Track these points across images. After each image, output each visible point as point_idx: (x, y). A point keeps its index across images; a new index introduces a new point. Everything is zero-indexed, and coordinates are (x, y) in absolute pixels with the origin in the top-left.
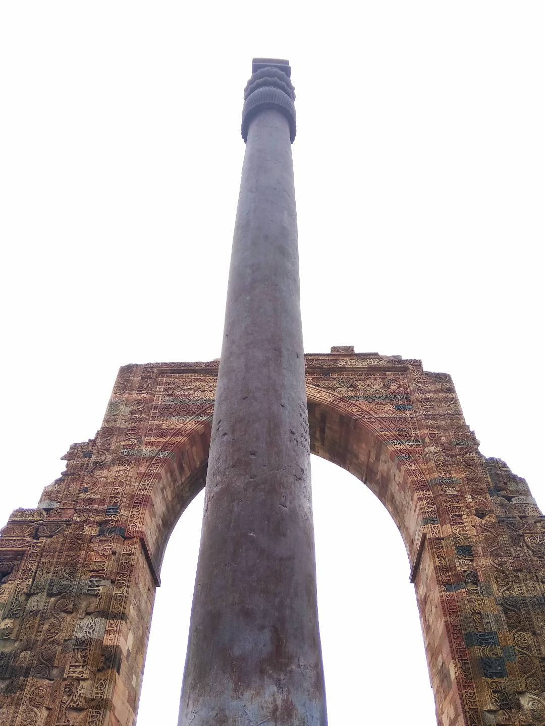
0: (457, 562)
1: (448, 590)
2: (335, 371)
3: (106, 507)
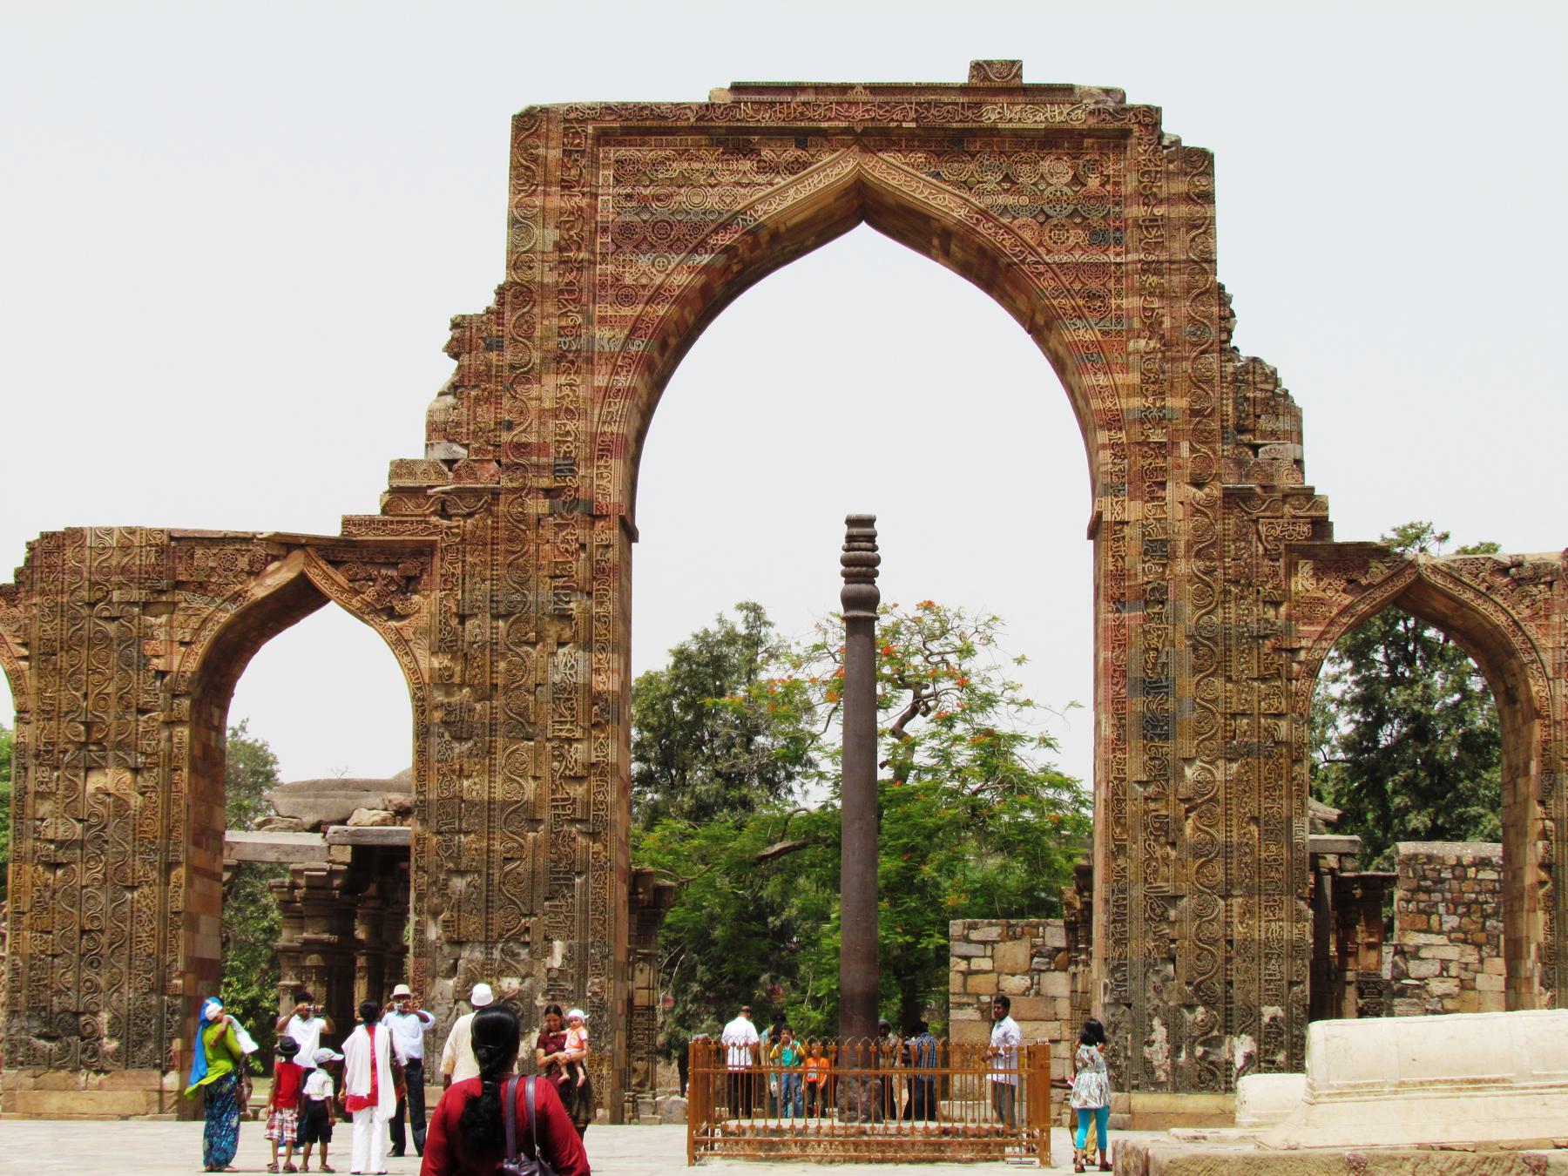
0: (1139, 567)
1: (1118, 610)
2: (975, 136)
3: (551, 460)
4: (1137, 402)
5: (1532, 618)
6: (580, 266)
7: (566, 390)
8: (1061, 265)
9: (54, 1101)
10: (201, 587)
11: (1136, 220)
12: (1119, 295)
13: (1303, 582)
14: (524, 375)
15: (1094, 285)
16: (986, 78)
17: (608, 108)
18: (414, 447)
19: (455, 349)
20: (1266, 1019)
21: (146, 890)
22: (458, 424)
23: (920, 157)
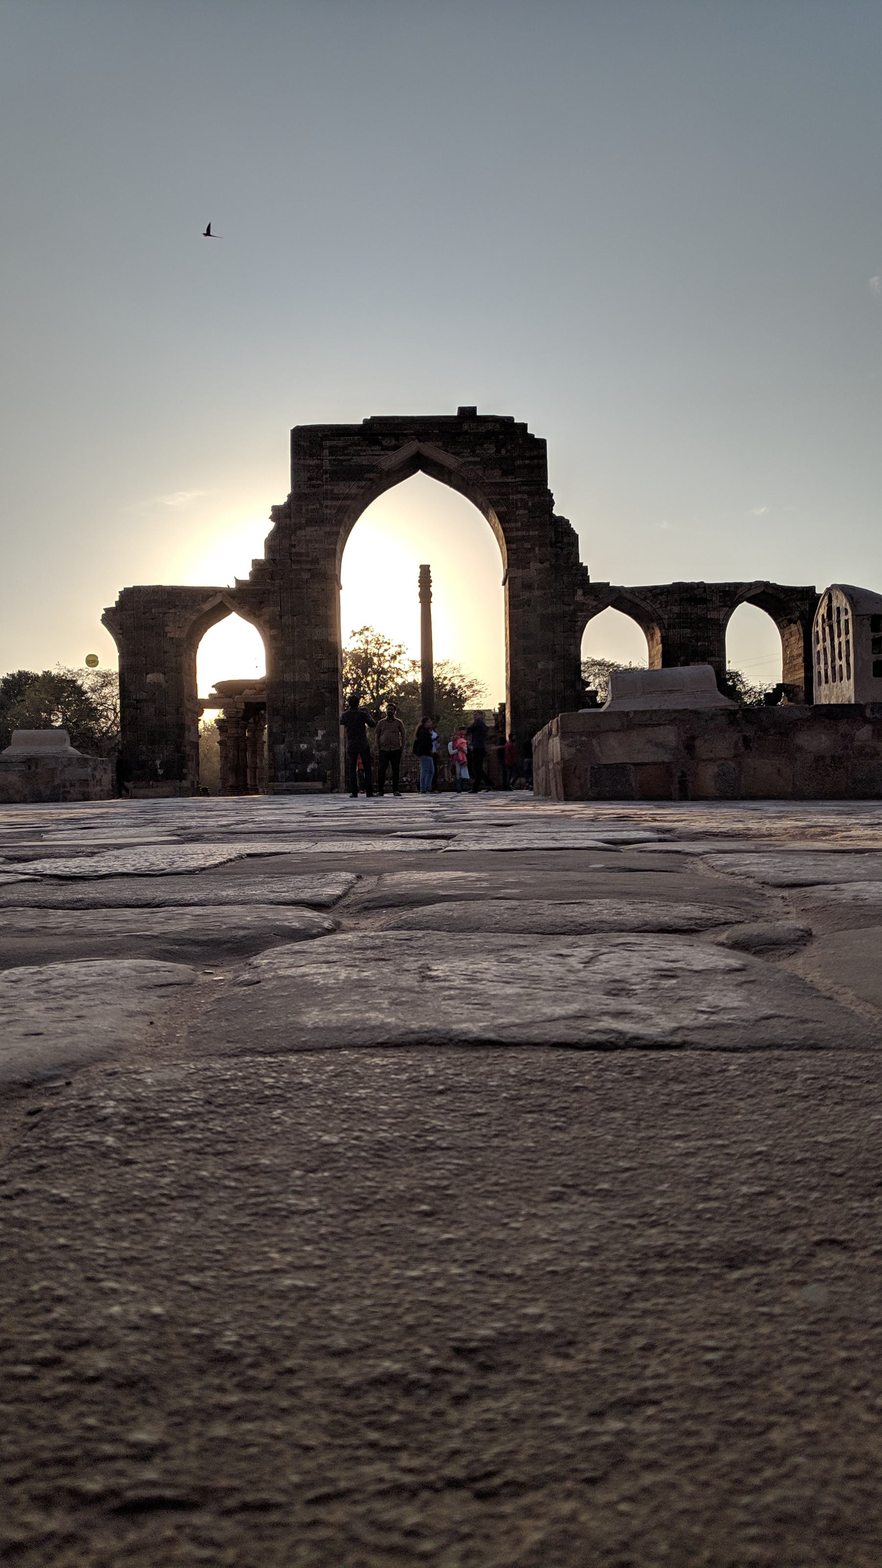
4: (519, 533)
6: (318, 486)
9: (142, 792)
10: (185, 607)
13: (579, 596)
15: (504, 490)
18: (261, 555)
19: (273, 518)
23: (440, 444)
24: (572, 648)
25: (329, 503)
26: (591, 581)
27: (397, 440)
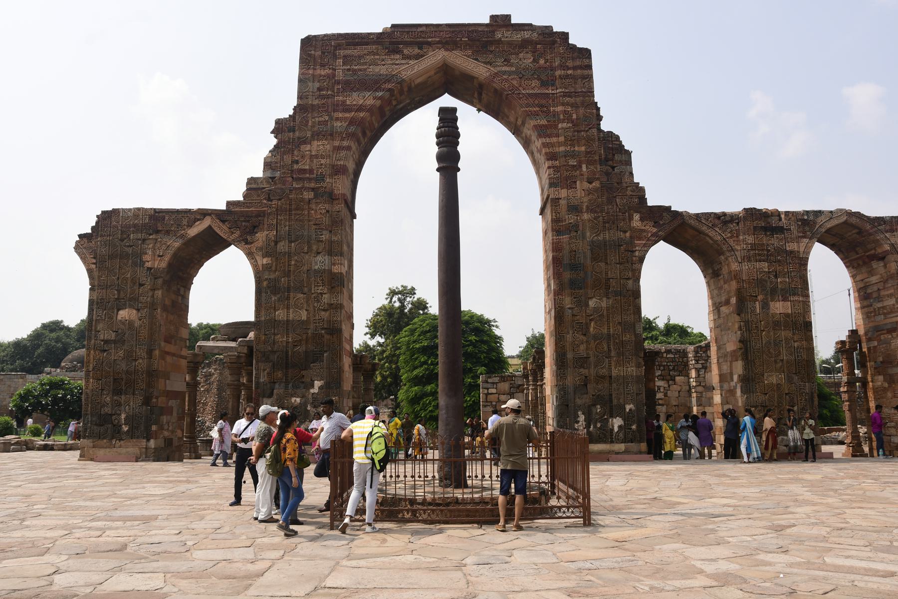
3: (315, 176)
4: (562, 149)
5: (731, 237)
6: (328, 97)
7: (321, 147)
8: (529, 94)
9: (101, 452)
10: (168, 232)
11: (560, 76)
12: (554, 106)
13: (636, 221)
14: (304, 141)
15: (543, 102)
16: (496, 21)
17: (340, 35)
18: (258, 172)
20: (627, 410)
21: (141, 361)
22: (276, 163)
23: (470, 52)
24: (630, 282)
25: (340, 115)
26: (649, 204)
27: (420, 48)
